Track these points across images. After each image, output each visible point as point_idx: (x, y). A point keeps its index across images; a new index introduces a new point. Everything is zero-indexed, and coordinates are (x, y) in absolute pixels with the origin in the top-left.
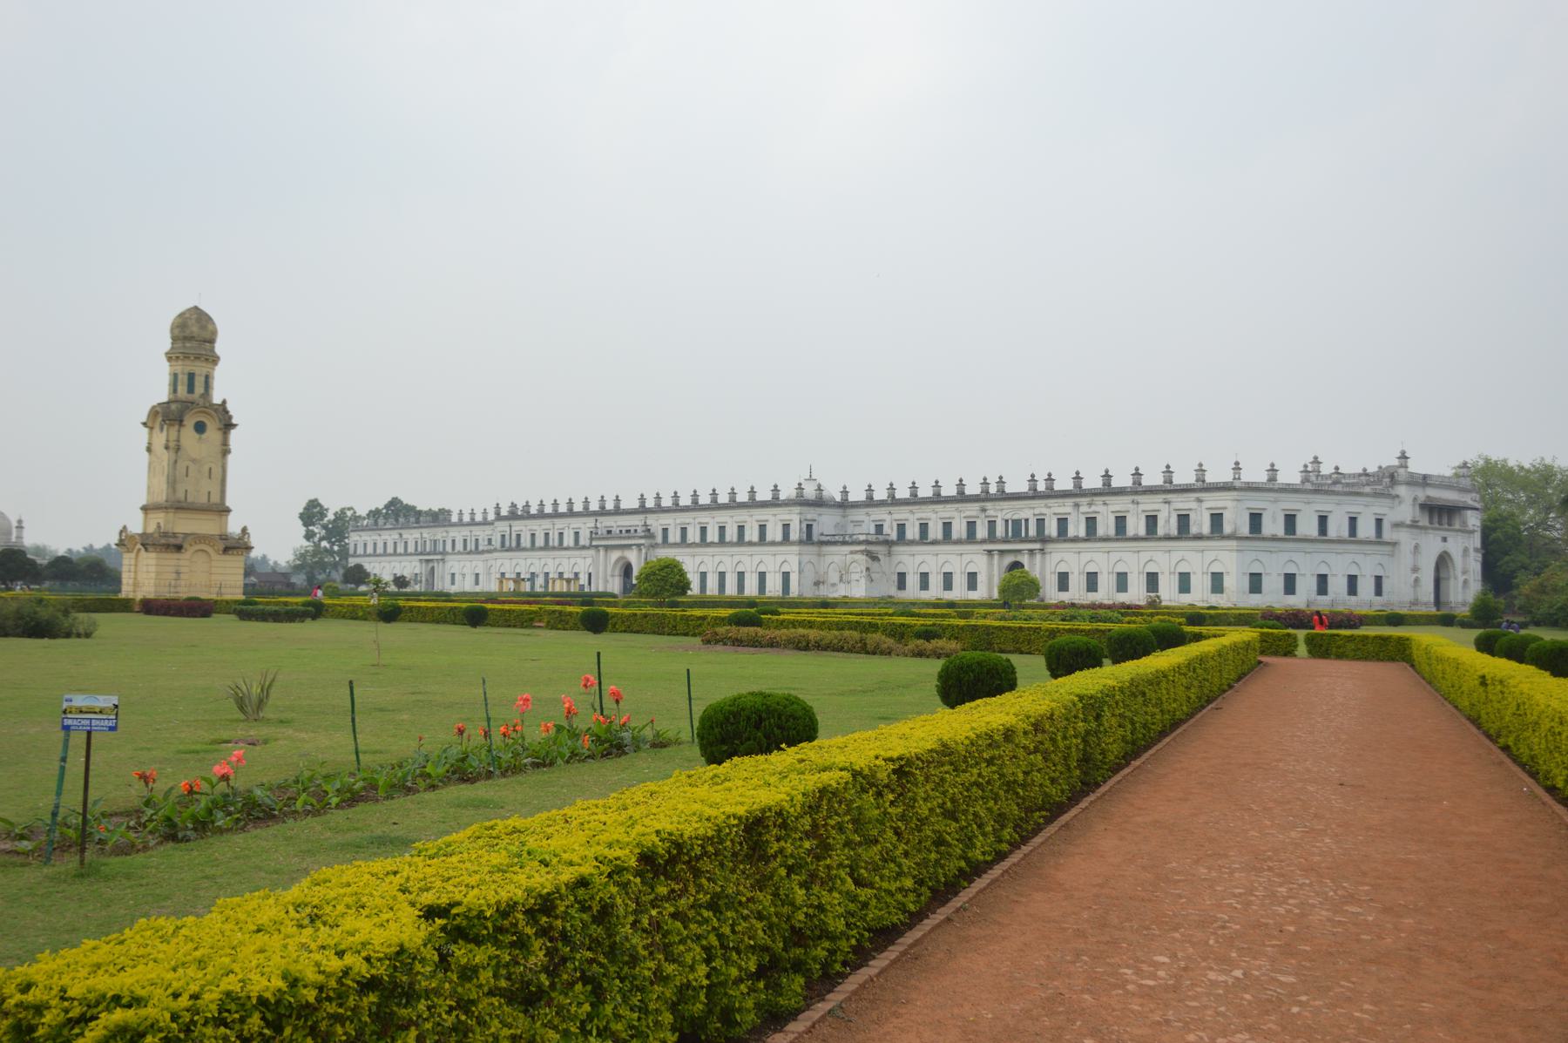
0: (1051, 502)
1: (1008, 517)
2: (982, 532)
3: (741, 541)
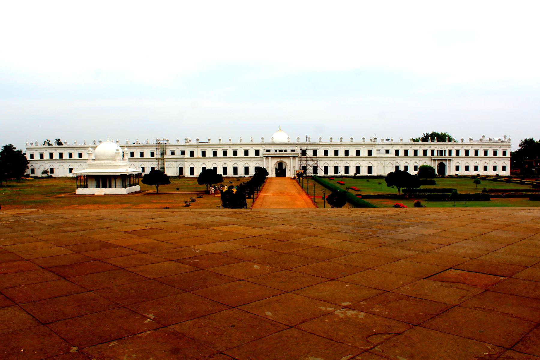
1: (439, 149)
2: (429, 154)
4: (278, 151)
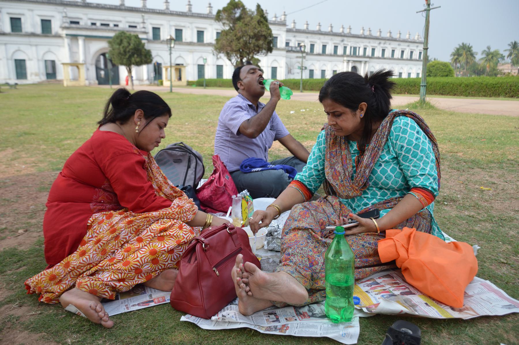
0: (371, 41)
2: (340, 51)
3: (372, 57)
4: (98, 24)
